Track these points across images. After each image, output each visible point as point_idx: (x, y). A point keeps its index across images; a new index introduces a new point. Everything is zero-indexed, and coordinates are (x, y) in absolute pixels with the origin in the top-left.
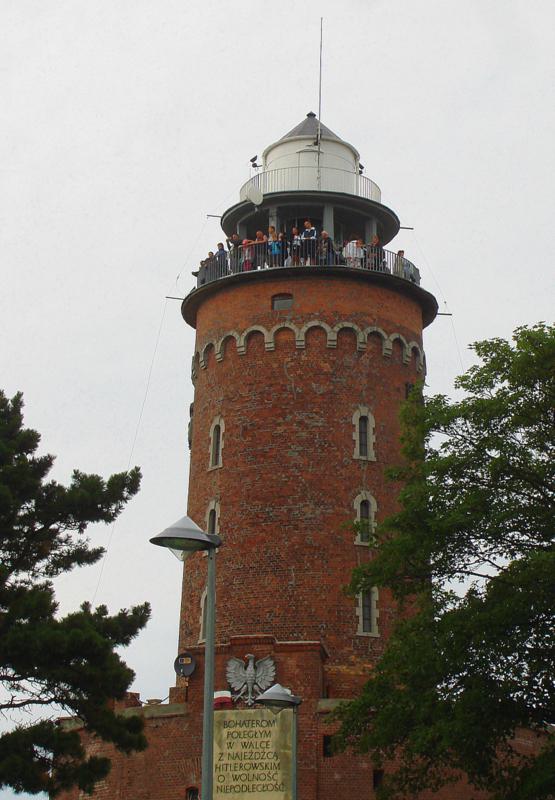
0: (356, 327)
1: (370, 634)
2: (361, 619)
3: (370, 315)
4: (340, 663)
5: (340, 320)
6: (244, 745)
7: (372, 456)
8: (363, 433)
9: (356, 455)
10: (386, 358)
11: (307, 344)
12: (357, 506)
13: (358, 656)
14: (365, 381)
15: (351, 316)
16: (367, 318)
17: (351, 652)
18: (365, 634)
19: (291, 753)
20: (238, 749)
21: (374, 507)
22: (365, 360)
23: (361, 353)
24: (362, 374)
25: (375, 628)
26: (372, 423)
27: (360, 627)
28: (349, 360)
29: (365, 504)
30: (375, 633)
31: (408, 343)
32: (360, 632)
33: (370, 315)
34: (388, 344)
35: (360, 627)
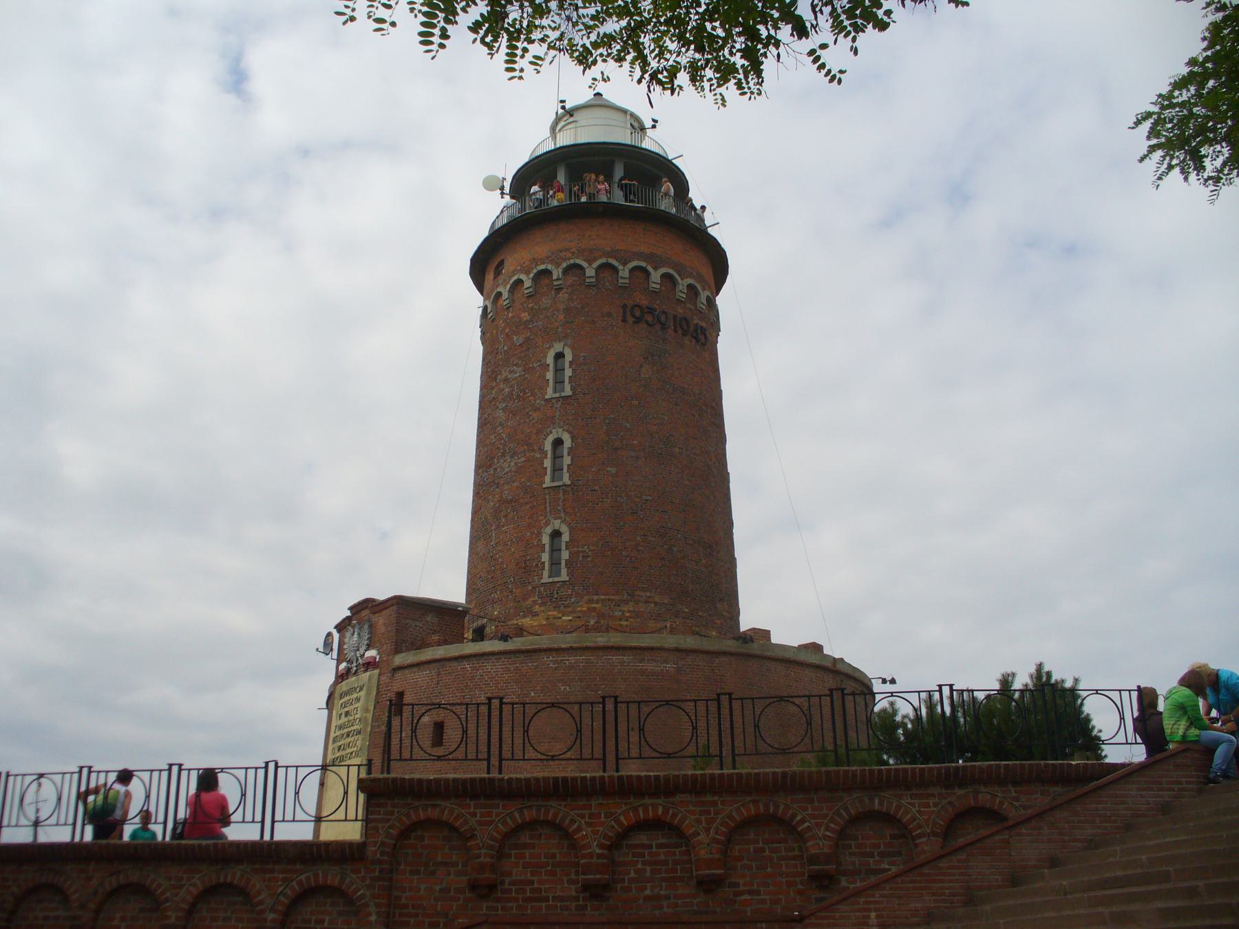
0: (549, 267)
1: (556, 579)
2: (547, 565)
3: (566, 250)
4: (524, 616)
5: (537, 265)
6: (347, 714)
7: (568, 391)
8: (559, 370)
9: (550, 393)
10: (589, 286)
11: (513, 301)
12: (548, 446)
13: (542, 604)
14: (562, 317)
15: (547, 257)
16: (562, 255)
17: (535, 603)
18: (551, 580)
19: (370, 716)
20: (344, 719)
21: (568, 443)
22: (563, 296)
23: (559, 290)
24: (558, 310)
25: (564, 572)
26: (569, 356)
27: (546, 573)
28: (546, 301)
29: (558, 443)
30: (564, 576)
31: (625, 264)
32: (546, 578)
33: (566, 250)
34: (656, 276)
35: (546, 573)
